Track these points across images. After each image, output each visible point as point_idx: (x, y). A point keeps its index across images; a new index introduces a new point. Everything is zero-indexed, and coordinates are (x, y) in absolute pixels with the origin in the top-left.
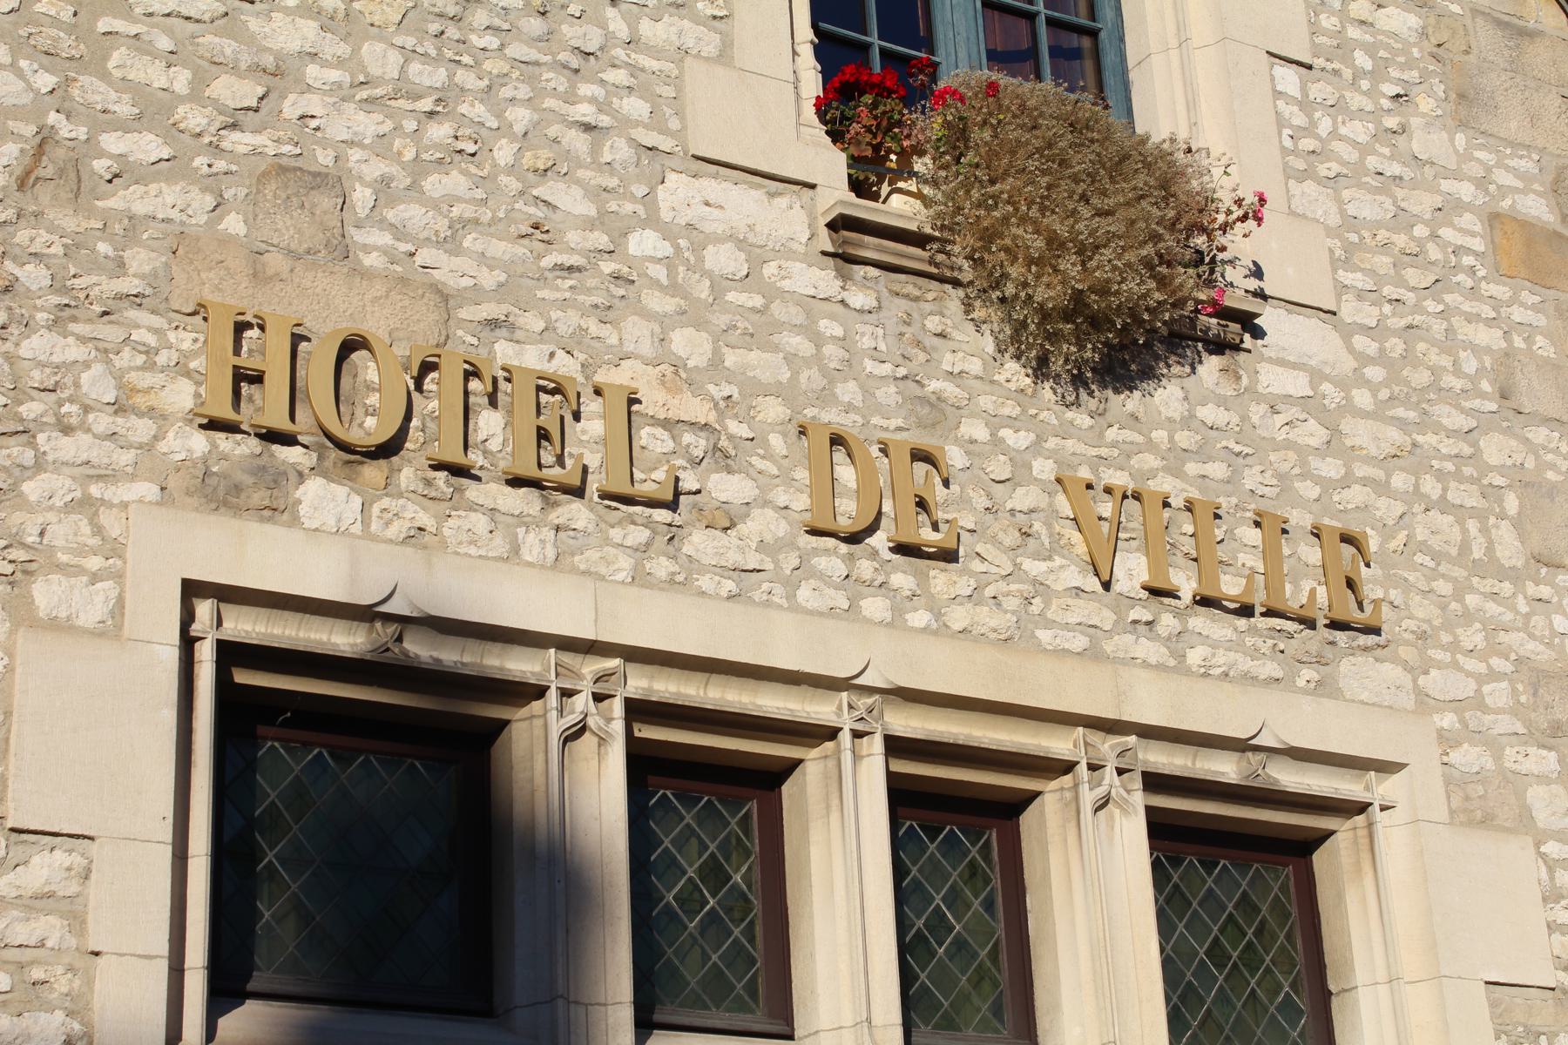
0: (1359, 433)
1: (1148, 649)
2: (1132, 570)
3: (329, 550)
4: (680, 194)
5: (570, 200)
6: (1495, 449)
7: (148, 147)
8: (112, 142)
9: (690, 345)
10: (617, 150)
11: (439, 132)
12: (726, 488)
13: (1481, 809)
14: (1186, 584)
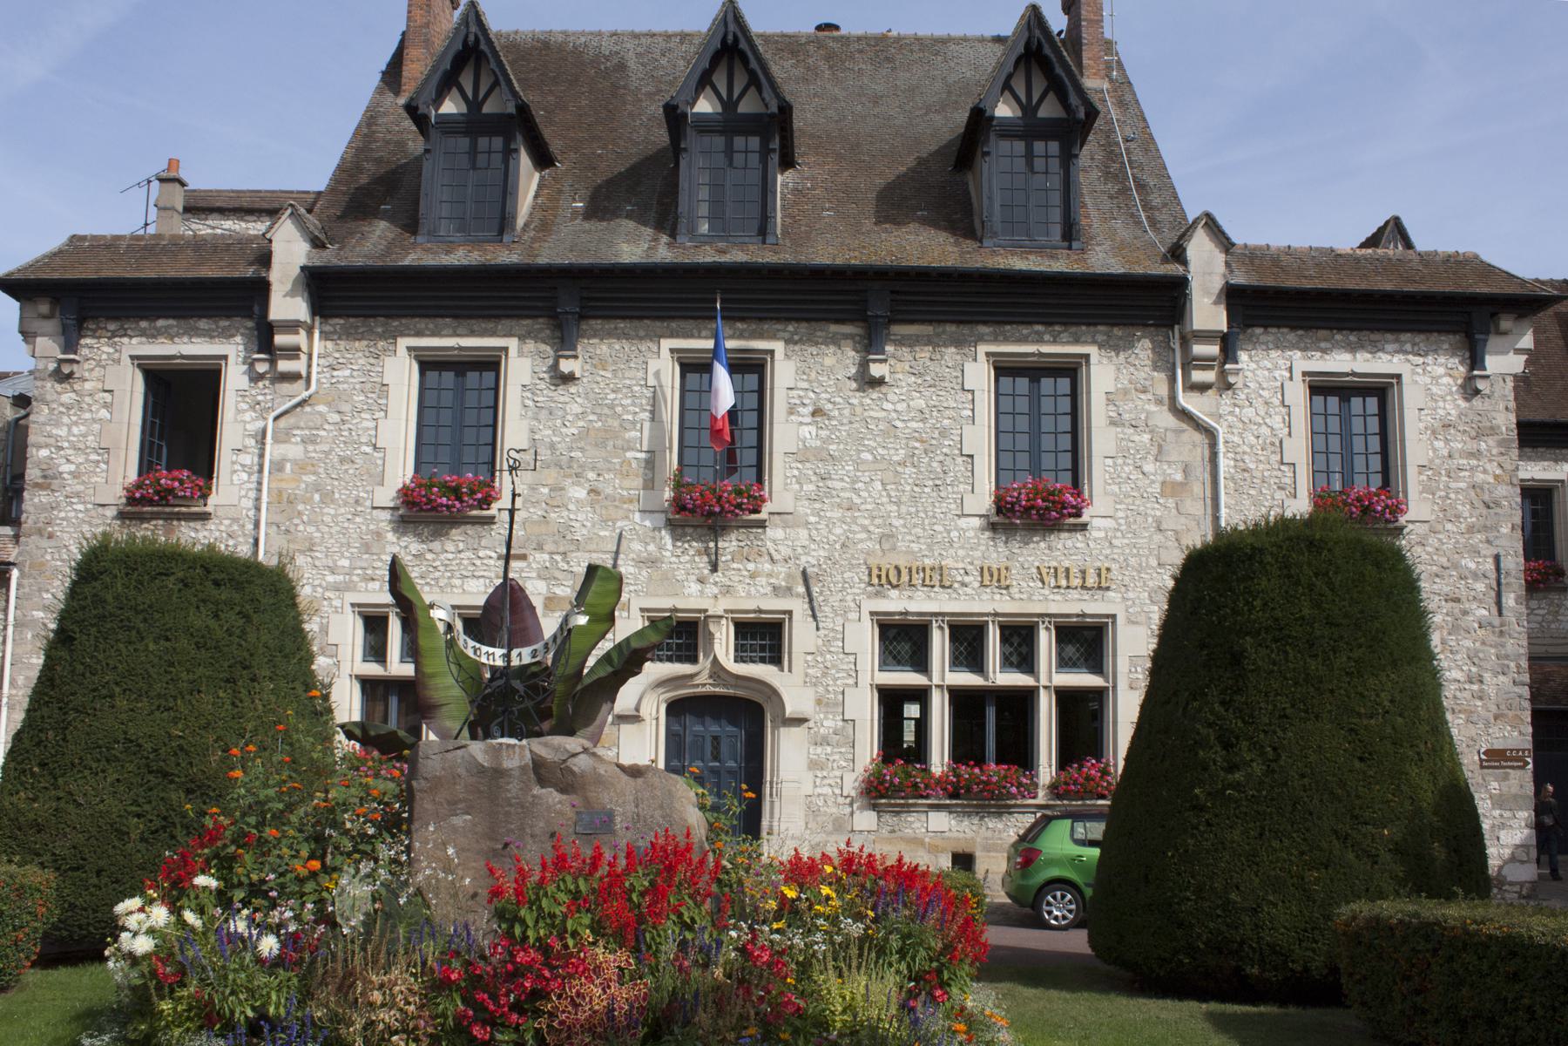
1: (1058, 597)
3: (896, 603)
5: (938, 528)
6: (1158, 538)
7: (864, 536)
9: (961, 553)
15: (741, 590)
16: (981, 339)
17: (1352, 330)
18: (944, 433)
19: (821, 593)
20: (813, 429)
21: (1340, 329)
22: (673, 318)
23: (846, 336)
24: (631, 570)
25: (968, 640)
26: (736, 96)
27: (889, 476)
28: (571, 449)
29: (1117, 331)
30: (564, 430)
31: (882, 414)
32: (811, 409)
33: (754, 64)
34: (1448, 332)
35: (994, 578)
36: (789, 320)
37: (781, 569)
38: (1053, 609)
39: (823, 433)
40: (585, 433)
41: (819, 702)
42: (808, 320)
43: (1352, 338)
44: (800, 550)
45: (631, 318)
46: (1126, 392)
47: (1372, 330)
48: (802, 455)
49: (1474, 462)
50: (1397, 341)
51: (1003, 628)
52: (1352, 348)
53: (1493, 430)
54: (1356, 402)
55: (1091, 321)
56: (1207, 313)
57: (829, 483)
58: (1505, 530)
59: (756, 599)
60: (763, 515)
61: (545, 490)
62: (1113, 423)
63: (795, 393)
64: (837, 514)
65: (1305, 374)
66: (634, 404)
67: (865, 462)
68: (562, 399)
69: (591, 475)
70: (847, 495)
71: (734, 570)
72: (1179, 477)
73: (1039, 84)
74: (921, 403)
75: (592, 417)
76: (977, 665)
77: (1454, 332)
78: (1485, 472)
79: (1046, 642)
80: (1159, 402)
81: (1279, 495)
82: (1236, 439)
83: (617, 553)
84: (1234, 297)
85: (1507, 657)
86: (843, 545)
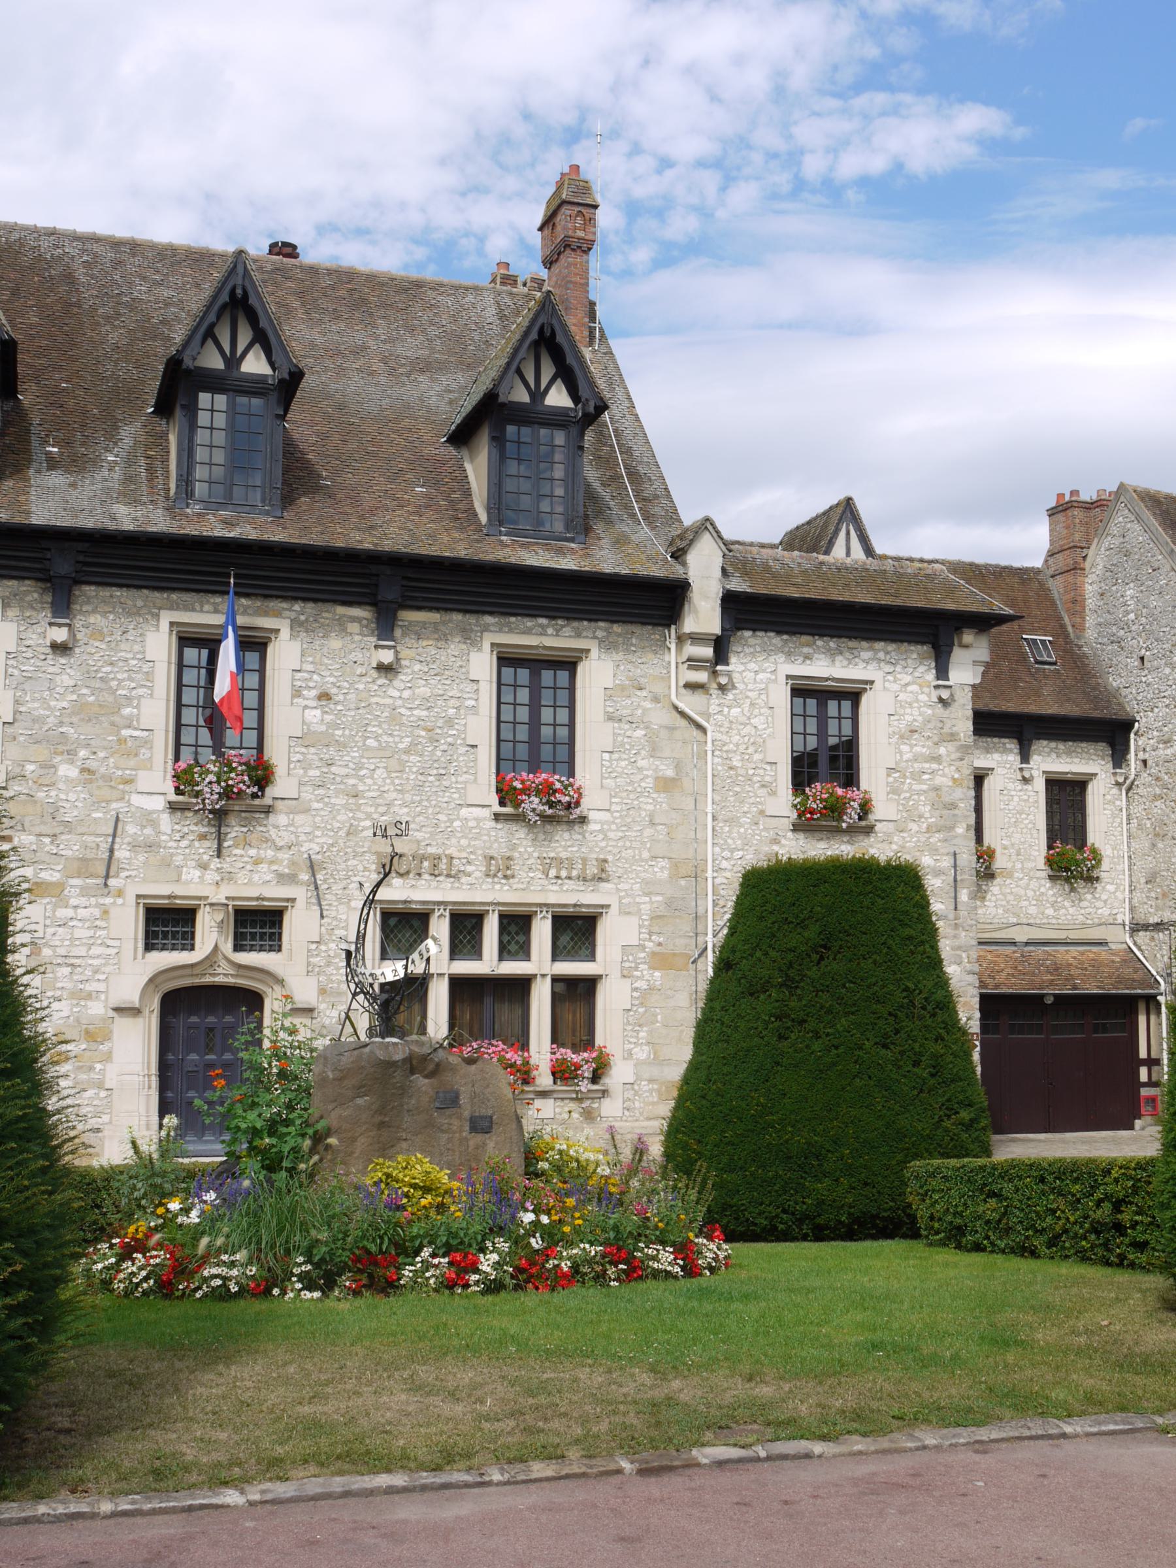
0: (611, 835)
1: (555, 888)
2: (553, 873)
3: (396, 892)
4: (464, 812)
5: (442, 817)
6: (648, 832)
8: (362, 824)
9: (464, 842)
10: (452, 805)
11: (418, 809)
12: (469, 868)
13: (624, 912)
14: (564, 874)
15: (242, 877)
16: (486, 629)
17: (832, 636)
18: (450, 723)
19: (325, 881)
20: (318, 712)
21: (821, 635)
22: (174, 589)
23: (354, 619)
24: (128, 854)
25: (466, 927)
26: (239, 353)
27: (393, 763)
28: (61, 723)
29: (617, 628)
30: (53, 703)
31: (388, 701)
32: (314, 693)
33: (263, 323)
34: (917, 642)
35: (500, 868)
36: (296, 599)
37: (284, 856)
38: (552, 899)
39: (328, 718)
40: (80, 708)
41: (322, 991)
42: (315, 600)
43: (832, 644)
44: (303, 838)
45: (128, 586)
46: (623, 688)
47: (850, 638)
48: (305, 739)
49: (935, 766)
50: (871, 649)
51: (502, 917)
52: (832, 654)
53: (953, 737)
54: (832, 706)
55: (593, 616)
56: (704, 614)
57: (333, 769)
58: (960, 830)
59: (256, 885)
60: (267, 801)
61: (30, 767)
62: (610, 718)
63: (298, 675)
64: (340, 801)
65: (788, 677)
66: (132, 680)
67: (369, 749)
68: (51, 670)
69: (82, 753)
70: (352, 781)
71: (238, 855)
72: (670, 773)
73: (548, 371)
74: (424, 691)
75: (85, 691)
76: (476, 952)
77: (923, 643)
78: (944, 775)
79: (542, 932)
80: (656, 699)
81: (762, 792)
82: (724, 738)
83: (114, 836)
84: (730, 600)
85: (959, 948)
86: (348, 834)
